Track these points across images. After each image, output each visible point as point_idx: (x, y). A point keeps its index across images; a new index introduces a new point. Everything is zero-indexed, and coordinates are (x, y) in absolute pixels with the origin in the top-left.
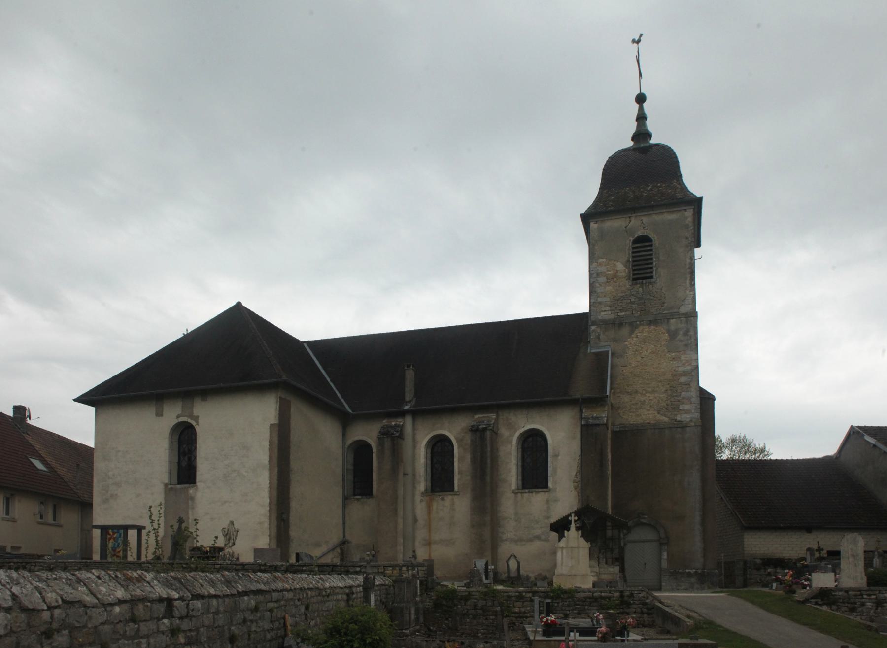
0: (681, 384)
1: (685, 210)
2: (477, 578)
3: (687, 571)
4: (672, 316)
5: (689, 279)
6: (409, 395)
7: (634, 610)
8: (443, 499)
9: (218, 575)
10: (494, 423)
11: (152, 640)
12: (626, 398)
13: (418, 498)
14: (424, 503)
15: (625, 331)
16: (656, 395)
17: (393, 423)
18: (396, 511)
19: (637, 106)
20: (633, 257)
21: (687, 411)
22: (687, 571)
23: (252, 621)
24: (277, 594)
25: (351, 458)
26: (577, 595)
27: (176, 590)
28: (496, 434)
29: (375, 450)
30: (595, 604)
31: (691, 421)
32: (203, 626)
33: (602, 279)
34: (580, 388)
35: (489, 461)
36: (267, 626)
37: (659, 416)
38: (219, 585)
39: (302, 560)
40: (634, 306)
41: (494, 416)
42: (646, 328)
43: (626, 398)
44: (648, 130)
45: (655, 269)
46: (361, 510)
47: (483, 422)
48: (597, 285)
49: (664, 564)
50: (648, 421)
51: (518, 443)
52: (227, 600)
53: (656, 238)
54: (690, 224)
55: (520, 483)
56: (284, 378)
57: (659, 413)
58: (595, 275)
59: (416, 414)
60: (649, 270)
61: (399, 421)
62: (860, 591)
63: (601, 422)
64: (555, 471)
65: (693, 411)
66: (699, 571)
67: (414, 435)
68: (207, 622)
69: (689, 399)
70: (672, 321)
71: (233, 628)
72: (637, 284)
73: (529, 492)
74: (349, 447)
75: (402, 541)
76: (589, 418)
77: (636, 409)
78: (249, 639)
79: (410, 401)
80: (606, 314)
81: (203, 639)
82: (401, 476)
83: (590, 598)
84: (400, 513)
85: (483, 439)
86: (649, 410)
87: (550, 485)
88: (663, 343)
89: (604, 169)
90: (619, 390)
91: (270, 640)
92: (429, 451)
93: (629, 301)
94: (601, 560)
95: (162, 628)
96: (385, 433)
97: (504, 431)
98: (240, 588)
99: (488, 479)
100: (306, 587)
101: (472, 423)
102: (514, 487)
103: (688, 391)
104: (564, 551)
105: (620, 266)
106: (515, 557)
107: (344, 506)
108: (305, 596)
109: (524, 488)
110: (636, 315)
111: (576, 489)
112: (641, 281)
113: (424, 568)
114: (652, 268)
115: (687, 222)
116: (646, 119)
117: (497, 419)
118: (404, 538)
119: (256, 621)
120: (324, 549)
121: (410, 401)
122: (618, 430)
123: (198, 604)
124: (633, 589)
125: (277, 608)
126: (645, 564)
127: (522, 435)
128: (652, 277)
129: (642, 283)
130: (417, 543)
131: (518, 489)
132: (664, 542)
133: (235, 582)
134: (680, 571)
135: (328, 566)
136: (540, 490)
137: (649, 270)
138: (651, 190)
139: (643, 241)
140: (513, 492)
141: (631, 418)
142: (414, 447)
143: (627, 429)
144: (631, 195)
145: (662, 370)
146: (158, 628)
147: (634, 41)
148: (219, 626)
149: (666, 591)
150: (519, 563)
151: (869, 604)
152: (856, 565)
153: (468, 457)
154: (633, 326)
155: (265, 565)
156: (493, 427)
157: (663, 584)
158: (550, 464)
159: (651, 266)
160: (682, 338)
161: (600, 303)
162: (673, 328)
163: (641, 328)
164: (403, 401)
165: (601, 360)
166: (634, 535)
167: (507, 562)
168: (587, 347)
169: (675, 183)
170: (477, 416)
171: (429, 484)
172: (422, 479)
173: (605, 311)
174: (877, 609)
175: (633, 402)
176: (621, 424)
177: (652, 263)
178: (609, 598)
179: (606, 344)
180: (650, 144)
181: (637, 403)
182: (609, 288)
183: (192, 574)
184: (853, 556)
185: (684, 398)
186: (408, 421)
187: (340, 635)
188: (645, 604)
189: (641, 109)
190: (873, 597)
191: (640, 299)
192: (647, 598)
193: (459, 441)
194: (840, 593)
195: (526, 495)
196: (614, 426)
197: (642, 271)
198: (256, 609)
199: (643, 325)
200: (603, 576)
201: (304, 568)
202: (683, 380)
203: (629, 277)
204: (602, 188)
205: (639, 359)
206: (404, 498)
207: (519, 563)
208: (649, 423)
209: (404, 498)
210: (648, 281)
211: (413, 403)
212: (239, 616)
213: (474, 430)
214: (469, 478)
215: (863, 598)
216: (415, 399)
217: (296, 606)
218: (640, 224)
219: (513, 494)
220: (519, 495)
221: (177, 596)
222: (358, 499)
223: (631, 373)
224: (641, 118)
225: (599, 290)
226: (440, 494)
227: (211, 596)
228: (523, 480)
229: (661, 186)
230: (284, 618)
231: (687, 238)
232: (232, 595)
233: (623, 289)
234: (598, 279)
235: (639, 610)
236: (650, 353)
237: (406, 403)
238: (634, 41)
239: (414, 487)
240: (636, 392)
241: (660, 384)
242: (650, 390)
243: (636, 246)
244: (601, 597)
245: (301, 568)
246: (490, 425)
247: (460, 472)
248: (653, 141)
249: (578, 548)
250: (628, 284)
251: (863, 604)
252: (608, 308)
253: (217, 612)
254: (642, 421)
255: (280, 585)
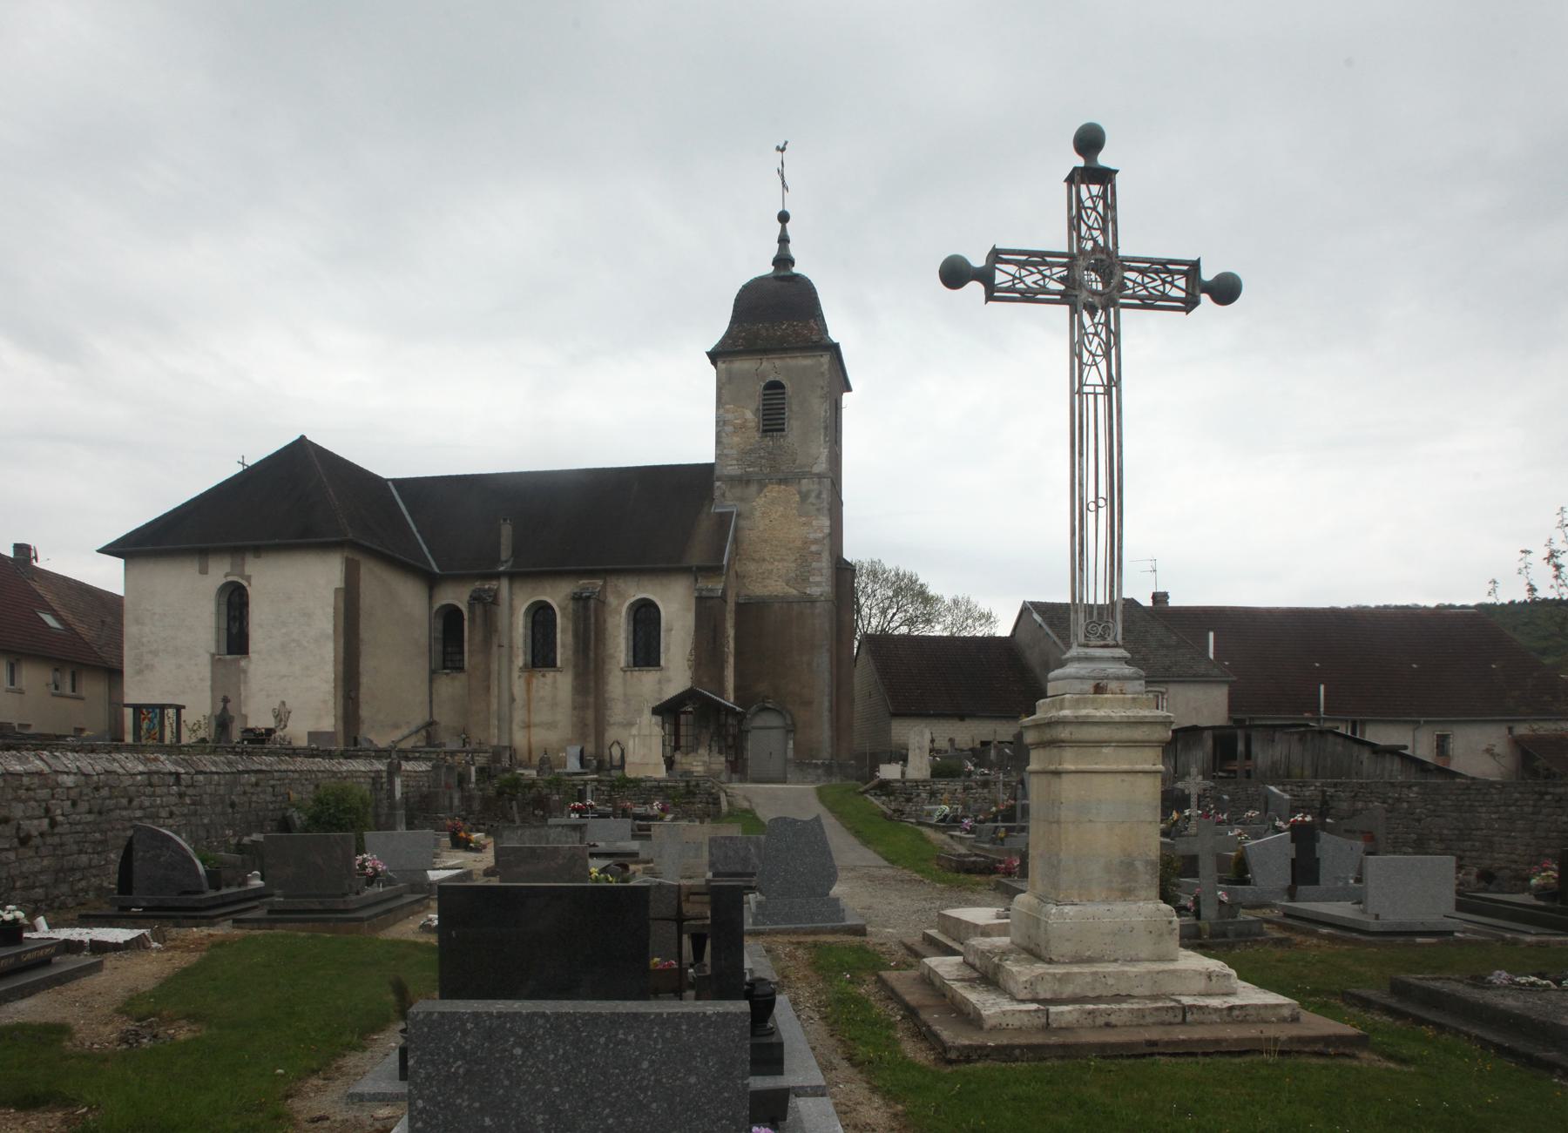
0: (812, 552)
1: (822, 356)
2: (547, 766)
3: (814, 761)
4: (804, 475)
5: (823, 434)
6: (505, 553)
7: (699, 800)
8: (544, 676)
9: (222, 758)
10: (599, 592)
11: (164, 799)
12: (752, 567)
13: (516, 674)
14: (522, 680)
15: (753, 488)
16: (785, 564)
17: (487, 587)
18: (488, 688)
19: (780, 225)
20: (764, 405)
21: (818, 584)
22: (814, 761)
23: (252, 794)
24: (279, 774)
25: (439, 625)
26: (643, 784)
27: (183, 767)
28: (604, 602)
29: (466, 617)
30: (661, 793)
31: (821, 595)
32: (206, 794)
33: (729, 429)
34: (697, 555)
35: (592, 634)
36: (269, 798)
37: (787, 587)
38: (221, 765)
39: (361, 744)
40: (763, 461)
41: (600, 582)
42: (776, 487)
43: (752, 567)
44: (790, 256)
45: (786, 420)
46: (449, 687)
47: (588, 589)
48: (724, 434)
49: (790, 754)
50: (775, 593)
51: (628, 613)
52: (227, 776)
53: (789, 385)
54: (827, 372)
55: (631, 659)
56: (350, 536)
57: (787, 585)
58: (721, 423)
59: (512, 576)
60: (780, 421)
61: (494, 584)
62: (916, 782)
63: (715, 595)
64: (668, 649)
65: (824, 584)
66: (827, 762)
67: (511, 600)
68: (209, 791)
69: (820, 570)
70: (804, 481)
71: (233, 797)
72: (766, 436)
73: (639, 670)
74: (437, 612)
75: (497, 723)
76: (703, 590)
77: (764, 579)
78: (250, 806)
79: (506, 562)
80: (733, 469)
81: (207, 802)
82: (495, 648)
83: (656, 787)
84: (494, 691)
85: (586, 608)
86: (777, 581)
87: (662, 663)
88: (793, 506)
89: (736, 300)
90: (745, 557)
91: (272, 810)
92: (530, 620)
93: (757, 455)
94: (713, 748)
95: (172, 792)
96: (476, 599)
97: (612, 600)
98: (240, 768)
99: (592, 655)
100: (315, 769)
101: (575, 591)
102: (622, 664)
103: (818, 562)
104: (637, 739)
105: (749, 415)
106: (619, 743)
107: (431, 681)
108: (313, 776)
109: (635, 665)
110: (765, 472)
111: (690, 668)
112: (771, 433)
113: (487, 755)
114: (784, 419)
115: (823, 370)
116: (789, 242)
117: (604, 587)
118: (499, 721)
119: (258, 794)
120: (405, 731)
121: (506, 562)
122: (743, 601)
123: (201, 778)
124: (699, 779)
125: (280, 785)
126: (771, 753)
127: (633, 604)
128: (783, 430)
129: (773, 436)
130: (515, 727)
131: (628, 666)
132: (791, 730)
133: (237, 764)
134: (807, 761)
135: (385, 751)
136: (651, 668)
137: (780, 421)
138: (786, 329)
139: (775, 387)
140: (622, 669)
141: (757, 590)
142: (511, 615)
143: (752, 601)
144: (764, 333)
145: (792, 536)
146: (169, 791)
147: (778, 149)
148: (220, 795)
149: (790, 783)
150: (623, 750)
151: (924, 795)
152: (921, 757)
153: (570, 626)
154: (762, 485)
155: (317, 749)
156: (598, 596)
157: (789, 776)
158: (662, 640)
159: (782, 416)
160: (814, 501)
161: (726, 455)
162: (804, 489)
163: (770, 487)
164: (497, 561)
165: (723, 520)
166: (759, 721)
167: (610, 749)
168: (711, 506)
169: (812, 323)
170: (581, 582)
171: (529, 658)
172: (521, 652)
173: (731, 465)
174: (930, 799)
175: (760, 571)
176: (746, 596)
177: (784, 414)
178: (674, 787)
179: (731, 503)
180: (792, 272)
181: (764, 573)
182: (736, 439)
183: (198, 757)
184: (919, 748)
185: (814, 569)
186: (504, 585)
187: (323, 805)
188: (710, 794)
189: (784, 229)
190: (928, 788)
191: (770, 453)
192: (713, 788)
193: (563, 609)
194: (898, 785)
195: (636, 674)
196: (738, 597)
197: (774, 422)
198: (257, 784)
199: (772, 484)
200: (713, 766)
201: (360, 753)
202: (814, 548)
203: (759, 428)
204: (732, 322)
205: (767, 522)
206: (499, 674)
207: (623, 750)
208: (776, 596)
209: (499, 674)
210: (779, 433)
211: (510, 564)
212: (239, 789)
213: (577, 598)
214: (570, 653)
215: (918, 789)
216: (512, 559)
217: (303, 785)
218: (772, 368)
219: (622, 673)
220: (629, 673)
221: (183, 771)
222: (447, 674)
223: (758, 537)
224: (784, 240)
225: (725, 440)
226: (541, 669)
227: (212, 773)
228: (635, 656)
229: (797, 325)
230: (289, 794)
231: (822, 388)
232: (233, 773)
233: (752, 441)
234: (726, 428)
235: (704, 800)
236: (780, 516)
237: (503, 563)
238: (778, 149)
239: (511, 661)
240: (764, 560)
241: (789, 552)
242: (778, 557)
243: (768, 392)
244: (667, 787)
245: (355, 753)
246: (594, 593)
247: (563, 646)
248: (796, 270)
249: (651, 735)
250: (757, 436)
251: (918, 795)
252: (735, 462)
253: (218, 784)
254: (769, 593)
255: (284, 767)
